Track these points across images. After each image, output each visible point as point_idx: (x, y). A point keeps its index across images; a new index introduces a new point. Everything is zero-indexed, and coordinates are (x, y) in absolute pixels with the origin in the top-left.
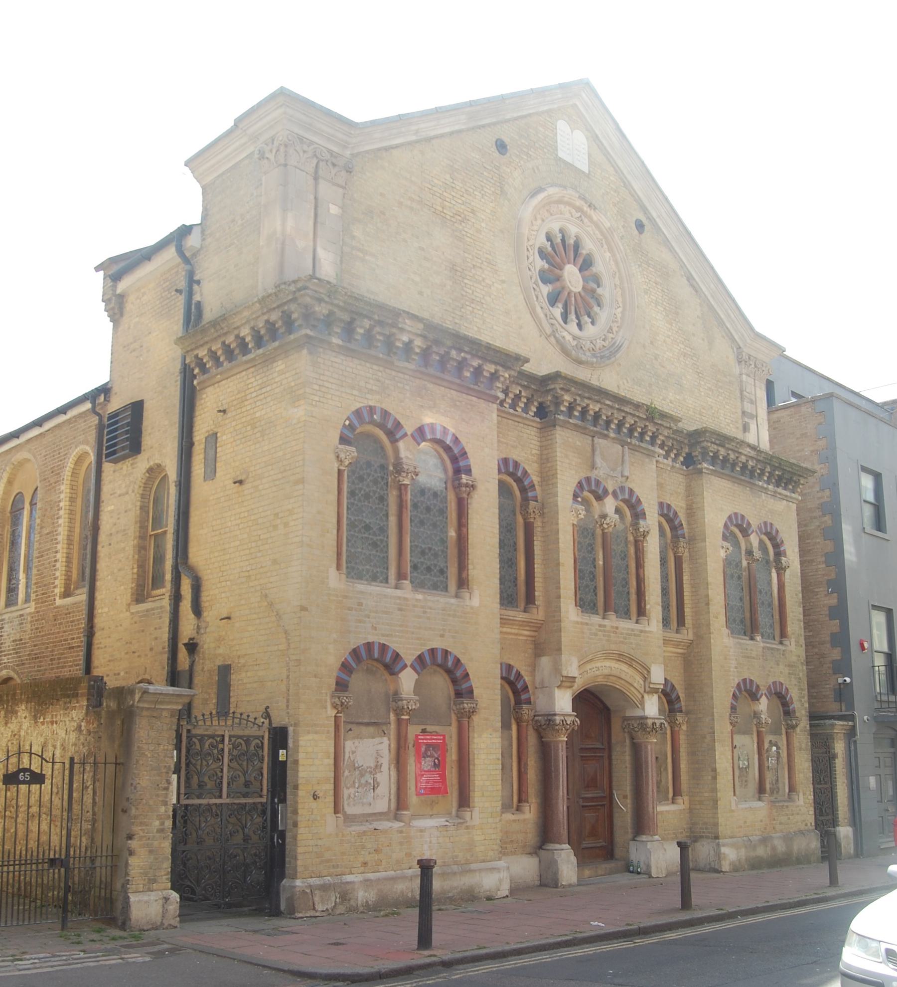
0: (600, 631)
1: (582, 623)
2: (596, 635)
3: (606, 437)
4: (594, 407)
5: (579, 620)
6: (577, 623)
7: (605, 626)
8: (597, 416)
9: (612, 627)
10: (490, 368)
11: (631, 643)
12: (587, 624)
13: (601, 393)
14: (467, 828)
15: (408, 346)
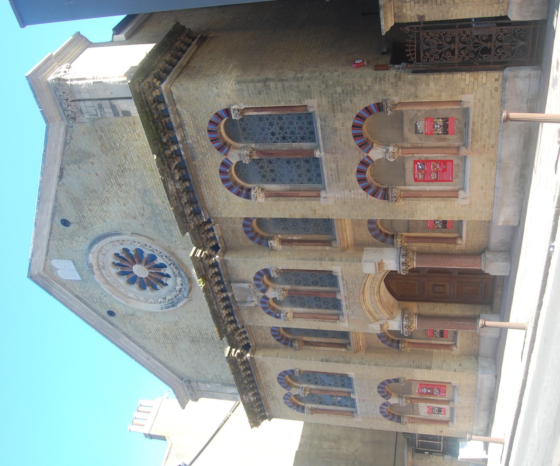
0: (350, 308)
1: (349, 320)
2: (353, 311)
3: (233, 296)
4: (224, 313)
5: (347, 321)
6: (349, 322)
7: (346, 305)
8: (226, 307)
9: (346, 300)
10: (242, 368)
11: (352, 287)
12: (348, 317)
13: (216, 316)
14: (460, 386)
15: (255, 395)
